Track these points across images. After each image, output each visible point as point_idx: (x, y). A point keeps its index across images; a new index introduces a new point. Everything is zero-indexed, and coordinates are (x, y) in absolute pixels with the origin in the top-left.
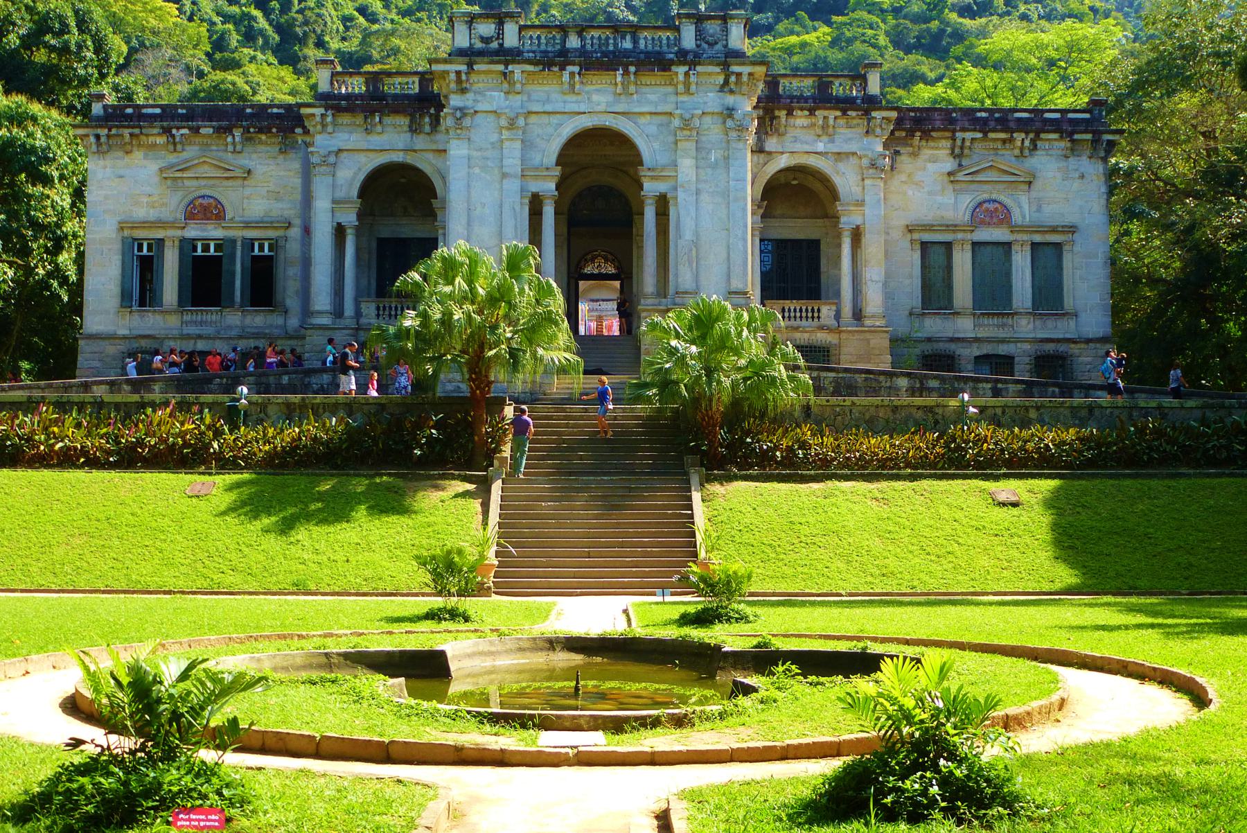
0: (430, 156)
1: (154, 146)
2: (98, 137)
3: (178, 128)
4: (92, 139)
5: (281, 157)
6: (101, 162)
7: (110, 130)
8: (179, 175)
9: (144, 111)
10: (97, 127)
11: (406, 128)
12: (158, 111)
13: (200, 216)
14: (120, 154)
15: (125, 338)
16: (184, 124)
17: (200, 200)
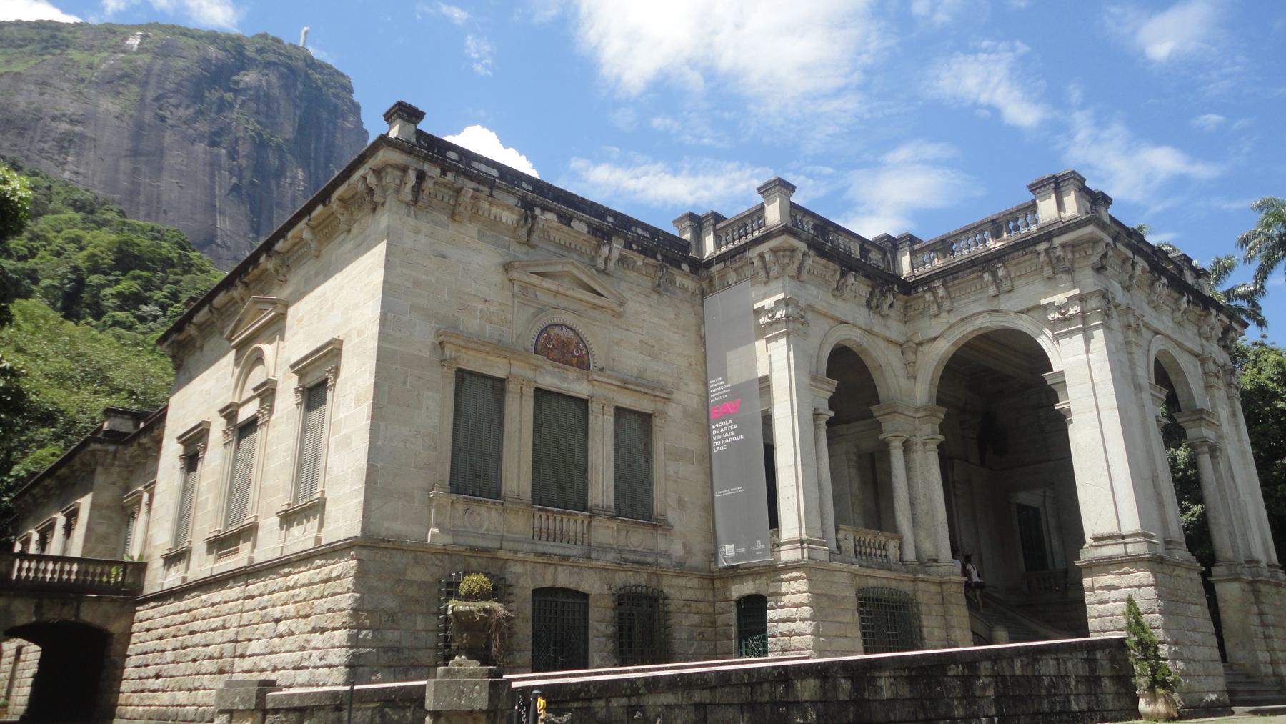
0: (881, 343)
1: (495, 223)
2: (421, 176)
3: (545, 209)
4: (412, 179)
5: (655, 296)
6: (411, 221)
7: (444, 173)
8: (536, 280)
9: (475, 164)
10: (425, 158)
11: (863, 301)
12: (494, 173)
13: (556, 354)
14: (444, 218)
15: (444, 552)
16: (555, 205)
17: (557, 329)
